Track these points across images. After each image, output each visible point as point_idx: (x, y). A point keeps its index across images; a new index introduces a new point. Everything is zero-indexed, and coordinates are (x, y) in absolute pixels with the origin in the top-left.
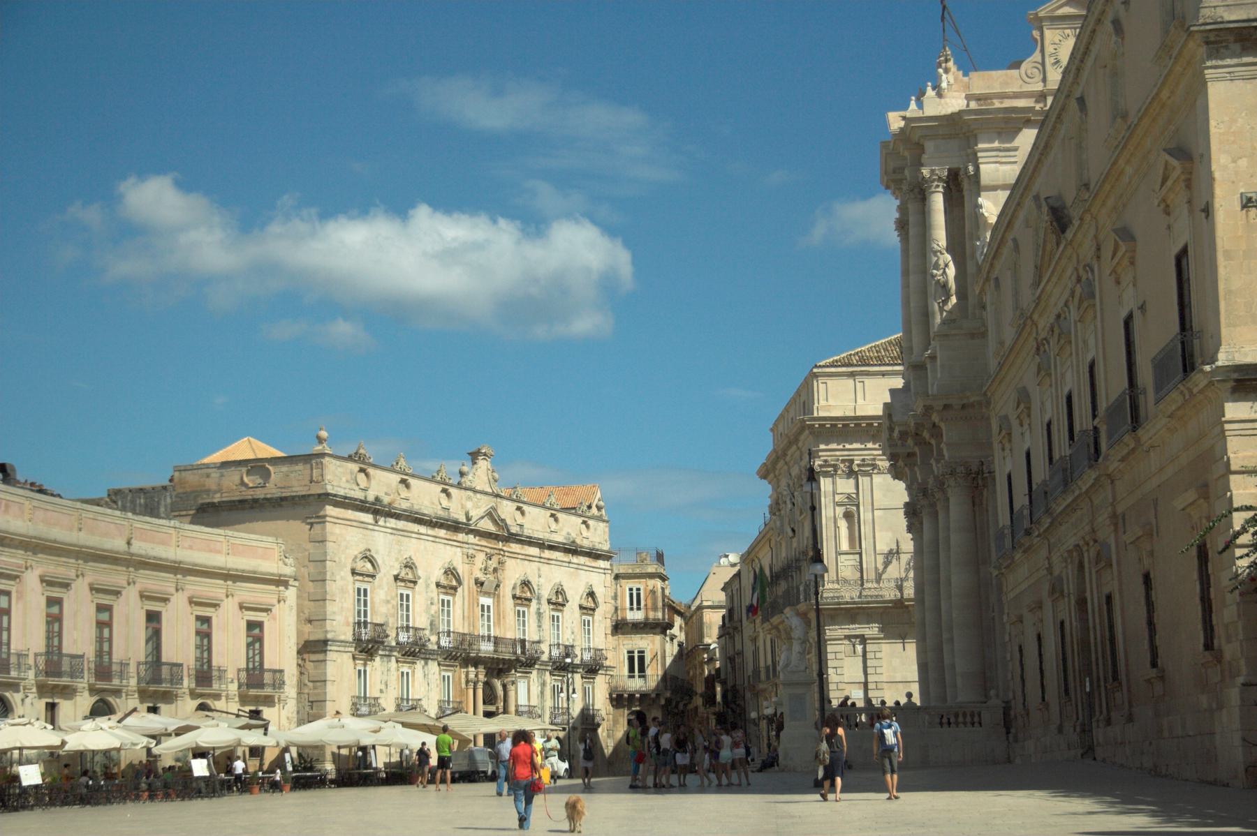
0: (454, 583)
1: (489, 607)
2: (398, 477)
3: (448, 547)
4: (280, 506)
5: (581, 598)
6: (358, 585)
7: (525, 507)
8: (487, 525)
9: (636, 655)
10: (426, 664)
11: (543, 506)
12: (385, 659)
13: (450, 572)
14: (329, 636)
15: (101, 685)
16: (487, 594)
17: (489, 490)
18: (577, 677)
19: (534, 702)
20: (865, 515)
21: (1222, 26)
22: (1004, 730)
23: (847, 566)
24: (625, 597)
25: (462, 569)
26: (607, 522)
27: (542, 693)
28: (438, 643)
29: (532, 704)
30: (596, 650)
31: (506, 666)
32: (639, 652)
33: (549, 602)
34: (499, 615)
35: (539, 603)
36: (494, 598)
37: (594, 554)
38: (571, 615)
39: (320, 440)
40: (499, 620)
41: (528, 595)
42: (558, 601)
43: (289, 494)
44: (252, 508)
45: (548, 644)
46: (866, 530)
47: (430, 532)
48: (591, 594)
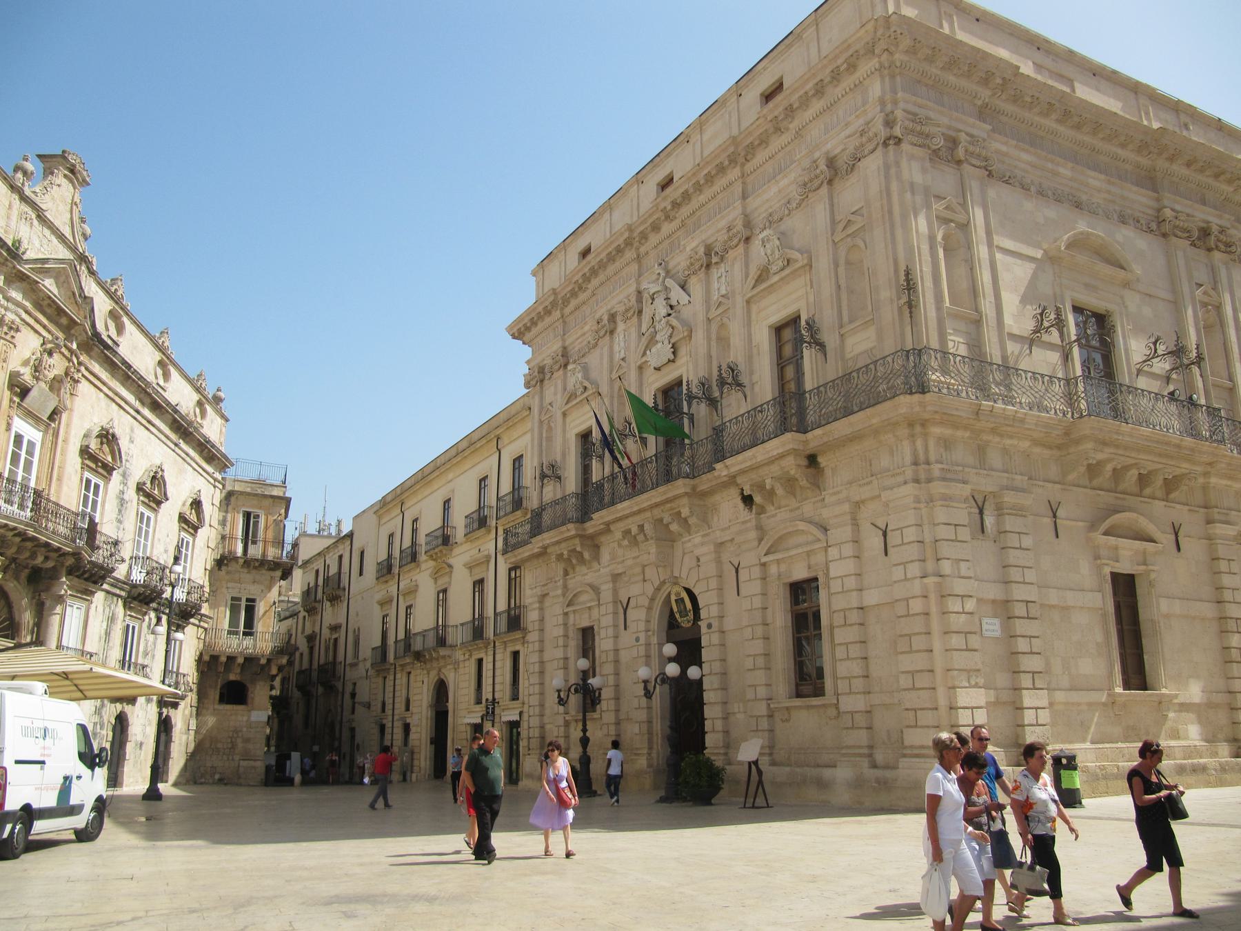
5: (184, 505)
9: (243, 603)
16: (31, 416)
20: (982, 251)
23: (957, 344)
24: (237, 525)
26: (227, 420)
27: (108, 634)
29: (88, 648)
31: (50, 564)
32: (248, 600)
33: (140, 488)
36: (46, 432)
37: (209, 453)
38: (167, 520)
46: (985, 277)
48: (197, 504)
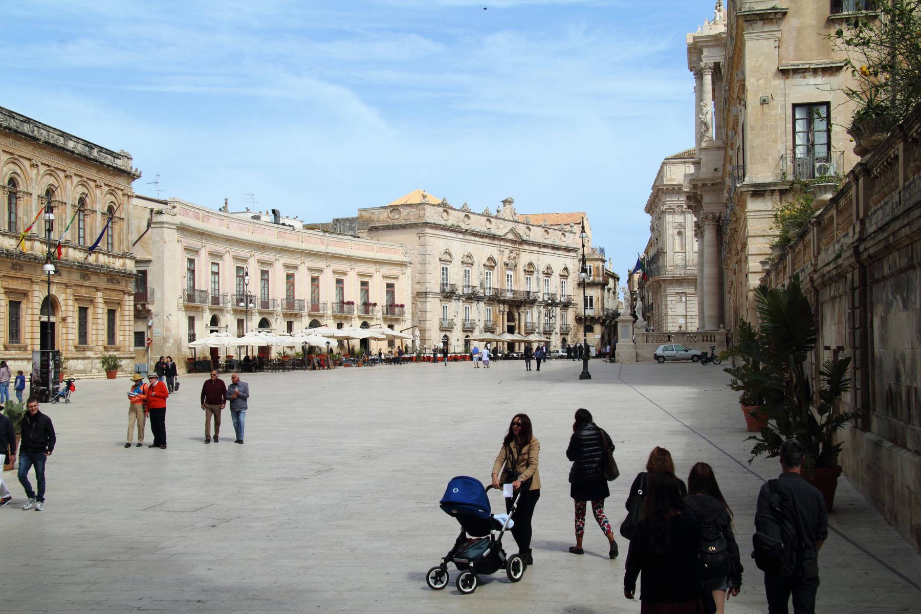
0: (493, 264)
1: (511, 276)
2: (464, 214)
3: (490, 247)
4: (406, 228)
6: (443, 266)
7: (531, 227)
8: (510, 236)
10: (478, 303)
11: (540, 226)
12: (457, 301)
13: (491, 259)
14: (428, 290)
15: (313, 313)
16: (511, 269)
17: (512, 219)
18: (558, 309)
19: (535, 320)
21: (752, 13)
22: (726, 344)
25: (497, 257)
27: (539, 316)
28: (484, 293)
30: (568, 296)
33: (543, 273)
34: (516, 279)
35: (538, 274)
38: (555, 280)
39: (424, 197)
40: (516, 282)
41: (532, 269)
42: (548, 273)
43: (409, 223)
44: (392, 229)
45: (542, 292)
47: (481, 240)
48: (566, 269)
